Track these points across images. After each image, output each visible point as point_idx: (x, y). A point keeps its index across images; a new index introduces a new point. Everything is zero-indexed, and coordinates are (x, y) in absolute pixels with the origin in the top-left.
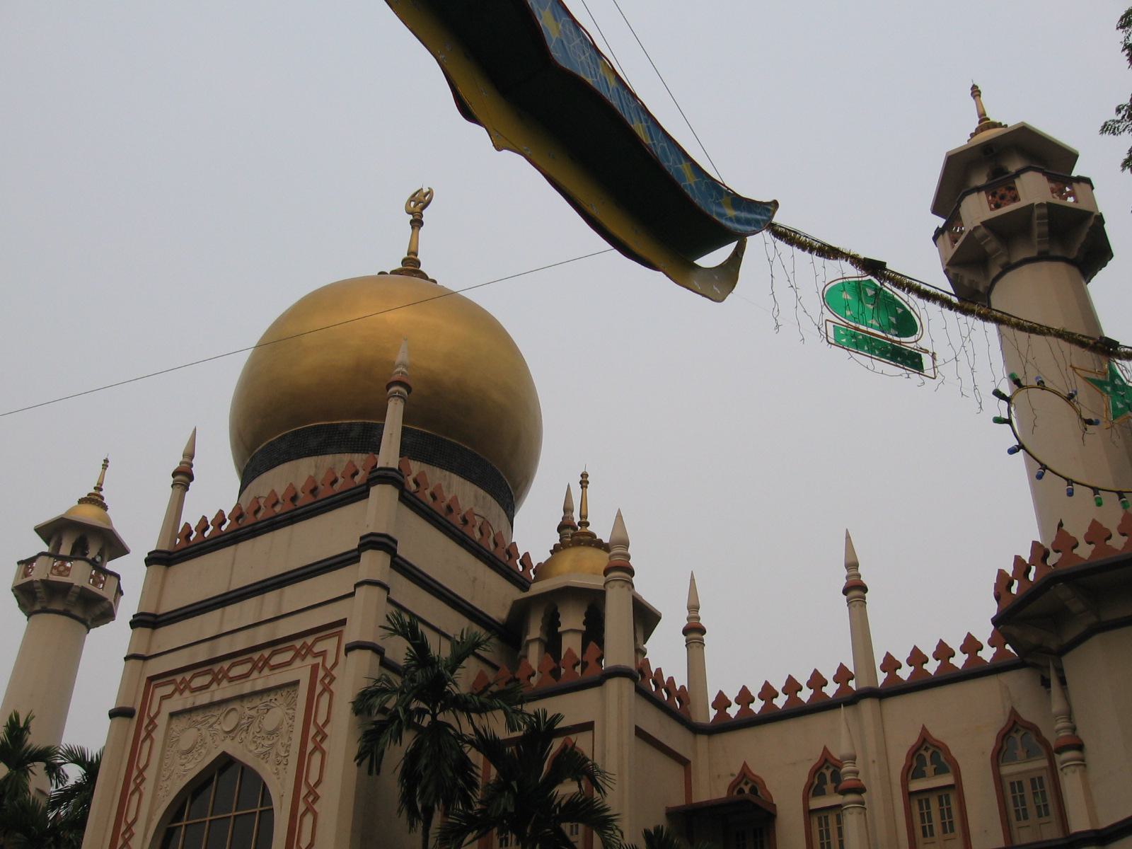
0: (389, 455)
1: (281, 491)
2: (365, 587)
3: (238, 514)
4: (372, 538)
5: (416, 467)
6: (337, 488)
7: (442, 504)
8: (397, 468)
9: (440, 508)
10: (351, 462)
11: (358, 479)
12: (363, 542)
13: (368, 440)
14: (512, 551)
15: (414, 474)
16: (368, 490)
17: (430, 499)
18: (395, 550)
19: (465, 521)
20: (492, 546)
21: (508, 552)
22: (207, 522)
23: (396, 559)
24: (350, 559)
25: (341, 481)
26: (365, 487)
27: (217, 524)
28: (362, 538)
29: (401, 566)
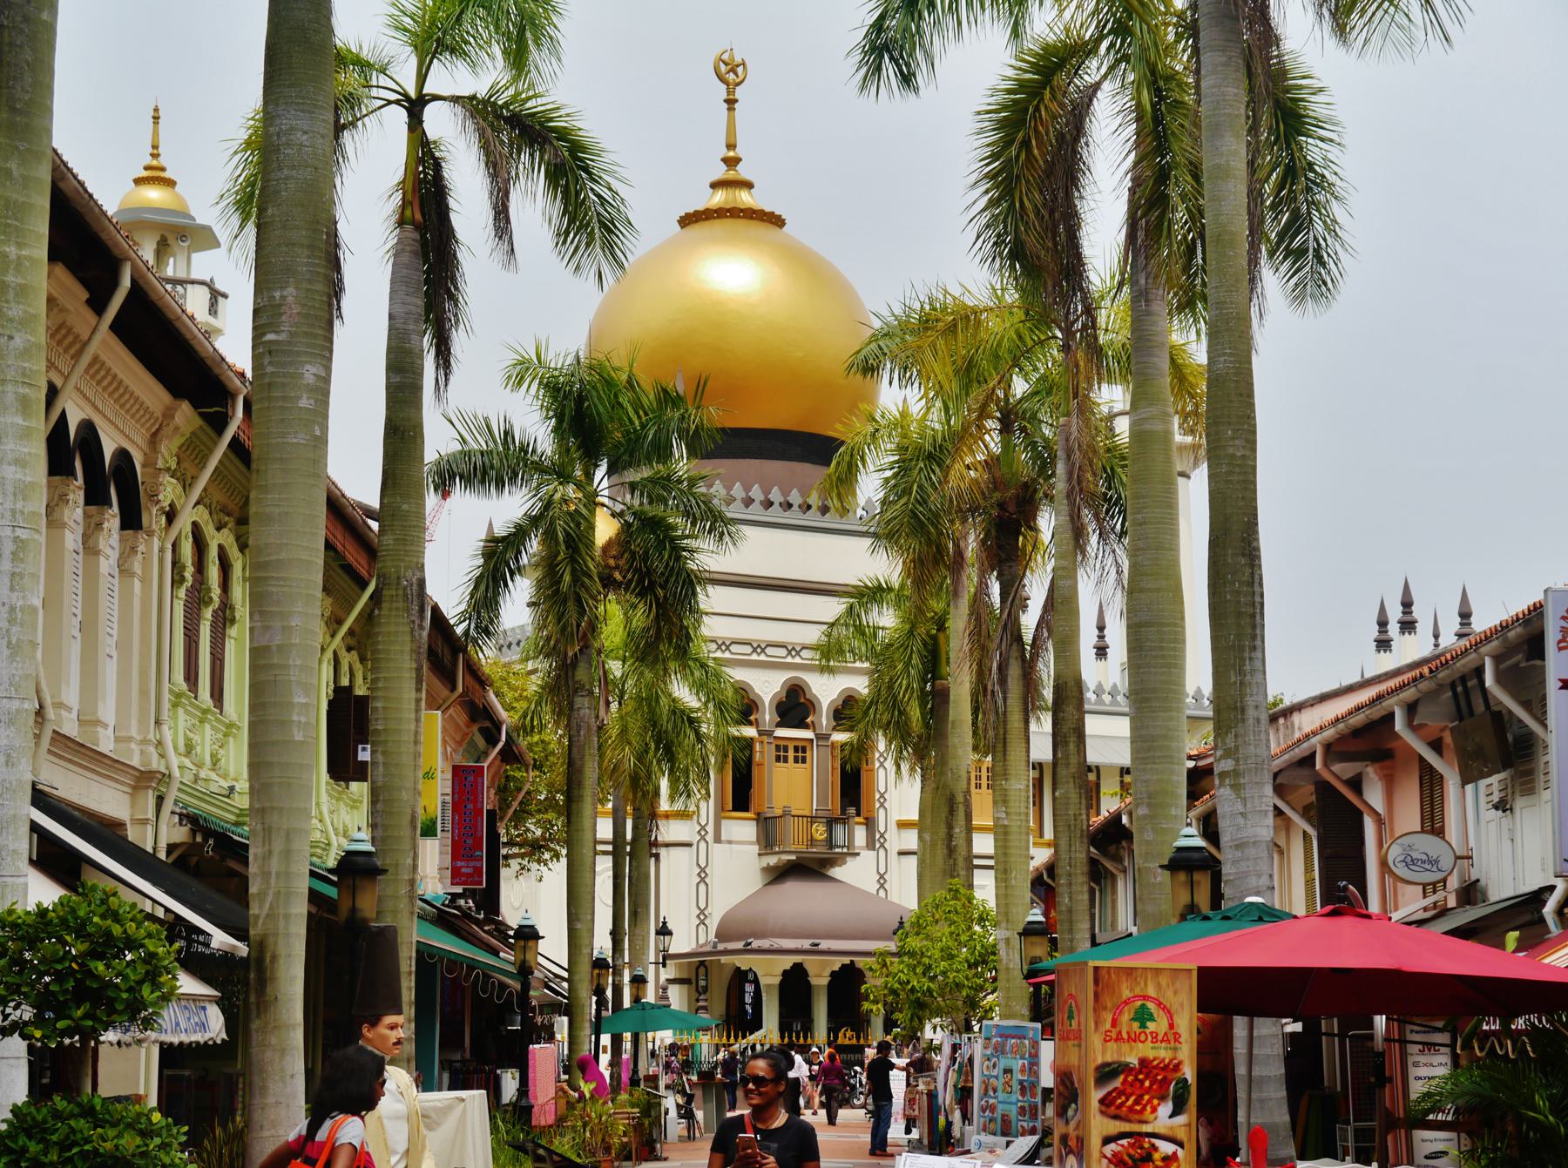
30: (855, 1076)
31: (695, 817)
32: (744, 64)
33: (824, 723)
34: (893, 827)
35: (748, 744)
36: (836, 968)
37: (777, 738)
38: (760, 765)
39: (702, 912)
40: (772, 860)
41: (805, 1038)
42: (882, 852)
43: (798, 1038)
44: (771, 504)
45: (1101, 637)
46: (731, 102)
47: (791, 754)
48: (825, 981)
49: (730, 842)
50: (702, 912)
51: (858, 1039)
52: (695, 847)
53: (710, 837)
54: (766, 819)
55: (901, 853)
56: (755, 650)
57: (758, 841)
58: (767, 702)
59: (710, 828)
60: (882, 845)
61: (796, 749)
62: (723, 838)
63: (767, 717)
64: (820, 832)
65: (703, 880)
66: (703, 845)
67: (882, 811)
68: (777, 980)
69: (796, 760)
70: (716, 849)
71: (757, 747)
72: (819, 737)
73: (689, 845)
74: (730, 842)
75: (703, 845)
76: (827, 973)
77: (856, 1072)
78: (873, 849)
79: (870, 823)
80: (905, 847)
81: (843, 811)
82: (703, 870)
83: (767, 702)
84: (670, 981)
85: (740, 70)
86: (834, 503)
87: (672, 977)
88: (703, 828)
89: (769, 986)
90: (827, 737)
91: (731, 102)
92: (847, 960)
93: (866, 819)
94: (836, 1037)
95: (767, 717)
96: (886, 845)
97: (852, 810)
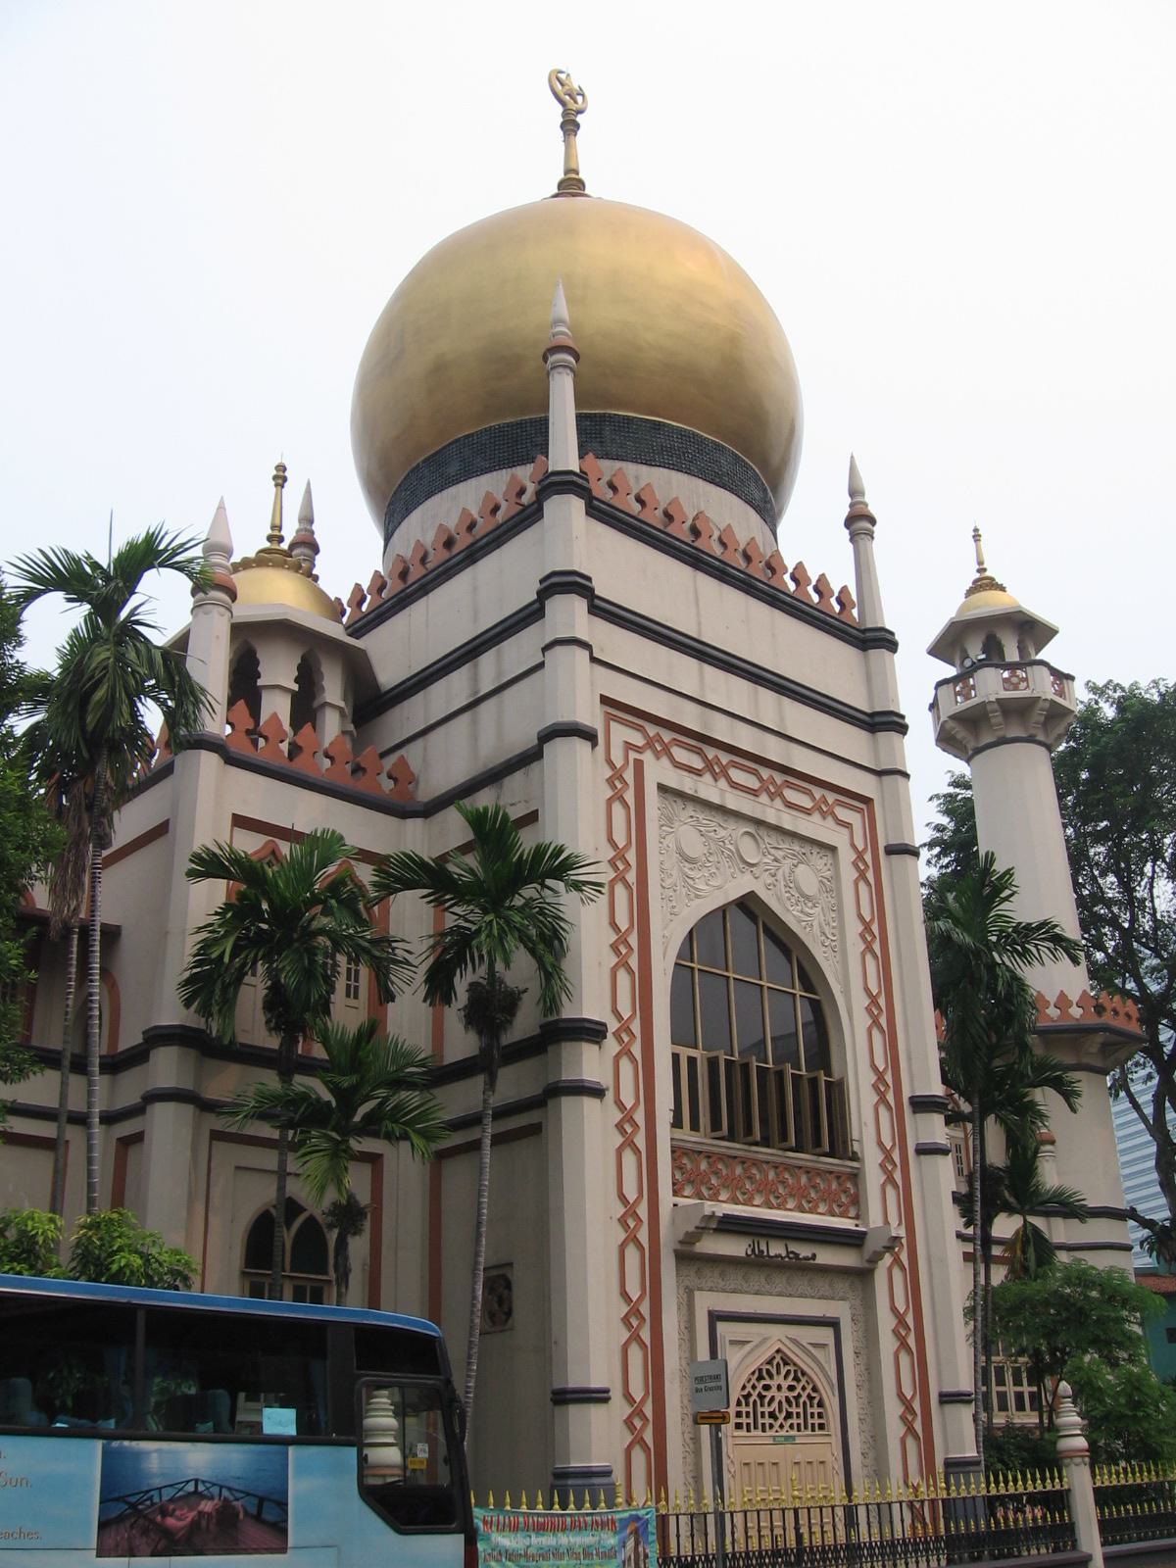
0: (564, 451)
1: (429, 538)
2: (558, 649)
3: (379, 584)
4: (555, 580)
5: (608, 467)
6: (500, 516)
7: (656, 511)
8: (578, 471)
9: (655, 518)
10: (513, 477)
11: (526, 499)
12: (545, 584)
13: (528, 438)
14: (773, 566)
15: (605, 479)
16: (540, 509)
17: (637, 507)
18: (592, 590)
19: (695, 532)
20: (742, 564)
21: (769, 566)
22: (342, 605)
23: (597, 602)
24: (532, 614)
25: (504, 505)
26: (536, 505)
27: (355, 604)
28: (541, 582)
29: (602, 610)
46: (570, 126)
73: (597, 1092)
80: (925, 1139)
91: (570, 126)
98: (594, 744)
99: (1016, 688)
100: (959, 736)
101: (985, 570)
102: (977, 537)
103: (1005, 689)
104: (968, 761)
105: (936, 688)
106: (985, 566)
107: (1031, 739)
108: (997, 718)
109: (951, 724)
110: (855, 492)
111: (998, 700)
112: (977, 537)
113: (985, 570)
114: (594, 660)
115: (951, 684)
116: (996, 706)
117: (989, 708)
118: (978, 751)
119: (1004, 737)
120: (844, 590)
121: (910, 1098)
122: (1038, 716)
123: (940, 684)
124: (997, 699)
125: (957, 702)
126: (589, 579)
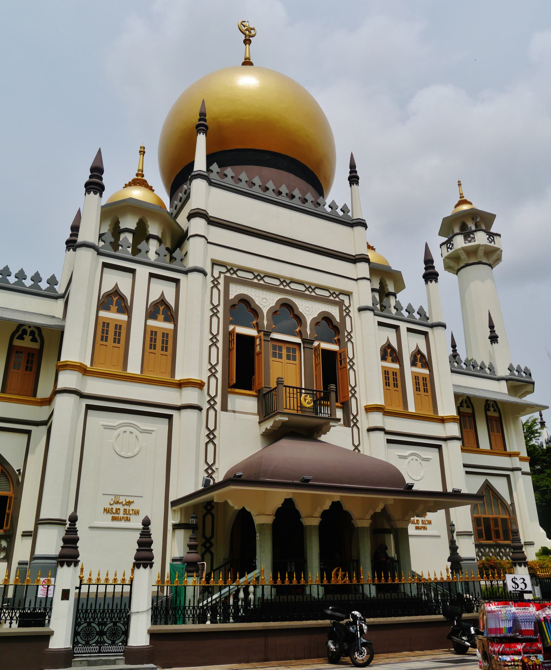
29: (212, 222)
30: (354, 623)
31: (206, 388)
32: (254, 29)
33: (309, 333)
34: (362, 411)
35: (251, 339)
36: (327, 506)
37: (273, 339)
38: (260, 353)
39: (210, 467)
40: (269, 424)
41: (299, 579)
42: (355, 429)
43: (291, 579)
44: (267, 189)
45: (454, 351)
46: (247, 41)
47: (284, 352)
48: (315, 522)
49: (234, 412)
50: (210, 467)
51: (351, 578)
52: (204, 411)
53: (218, 407)
54: (264, 395)
55: (370, 430)
56: (256, 277)
57: (259, 413)
58: (265, 312)
59: (218, 400)
60: (355, 424)
61: (288, 350)
62: (229, 408)
63: (265, 323)
64: (307, 401)
65: (211, 441)
66: (212, 412)
67: (353, 401)
68: (269, 520)
69: (288, 358)
70: (222, 415)
71: (258, 342)
72: (305, 341)
73: (199, 409)
74: (234, 412)
75: (212, 412)
76: (318, 513)
77: (355, 617)
78: (349, 426)
79: (346, 407)
81: (325, 386)
82: (211, 432)
83: (265, 312)
84: (176, 527)
85: (252, 31)
86: (309, 197)
87: (177, 522)
88: (212, 399)
89: (262, 525)
90: (312, 342)
91: (247, 41)
92: (337, 496)
93: (342, 403)
94: (329, 579)
95: (265, 323)
96: (358, 424)
97: (333, 386)
98: (205, 274)
99: (470, 242)
100: (451, 265)
101: (463, 197)
102: (460, 185)
103: (465, 243)
104: (457, 274)
105: (441, 248)
106: (463, 195)
107: (480, 263)
108: (463, 256)
109: (447, 260)
110: (353, 167)
111: (463, 249)
112: (460, 185)
113: (463, 197)
114: (208, 243)
115: (445, 245)
116: (462, 251)
117: (459, 252)
118: (459, 270)
119: (468, 263)
120: (345, 205)
121: (365, 407)
122: (481, 253)
123: (441, 245)
124: (461, 248)
125: (448, 251)
126: (205, 211)
